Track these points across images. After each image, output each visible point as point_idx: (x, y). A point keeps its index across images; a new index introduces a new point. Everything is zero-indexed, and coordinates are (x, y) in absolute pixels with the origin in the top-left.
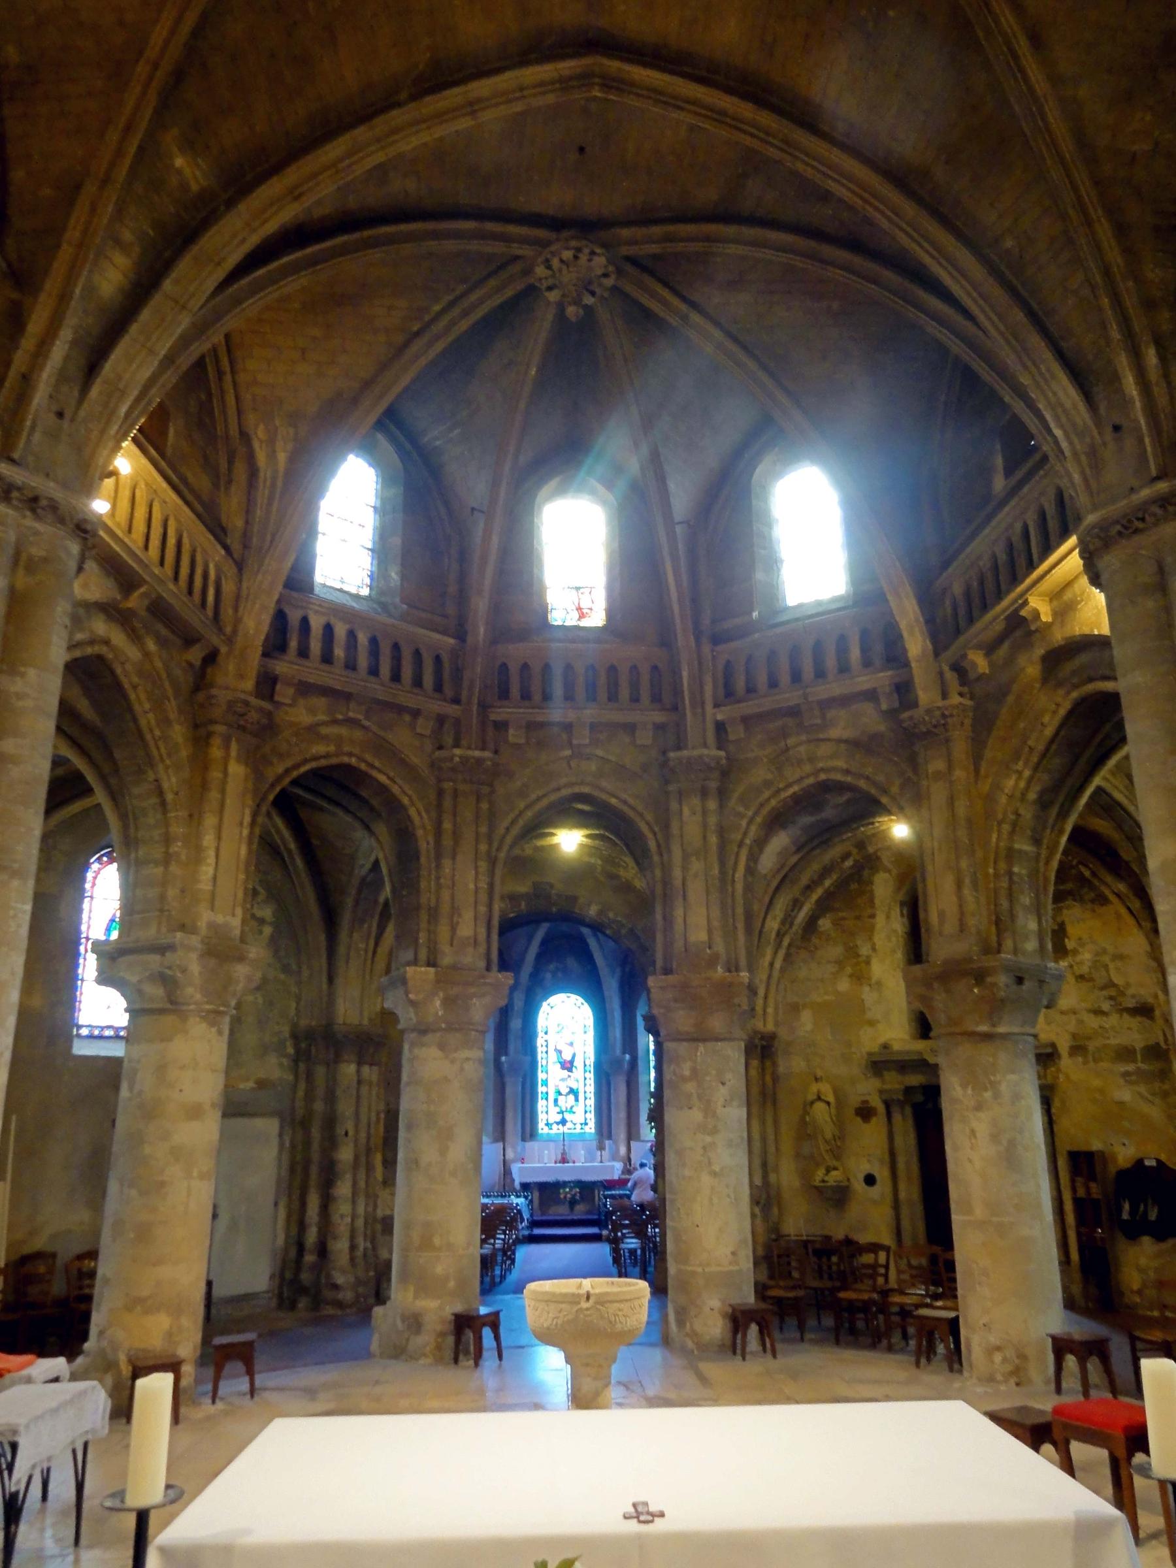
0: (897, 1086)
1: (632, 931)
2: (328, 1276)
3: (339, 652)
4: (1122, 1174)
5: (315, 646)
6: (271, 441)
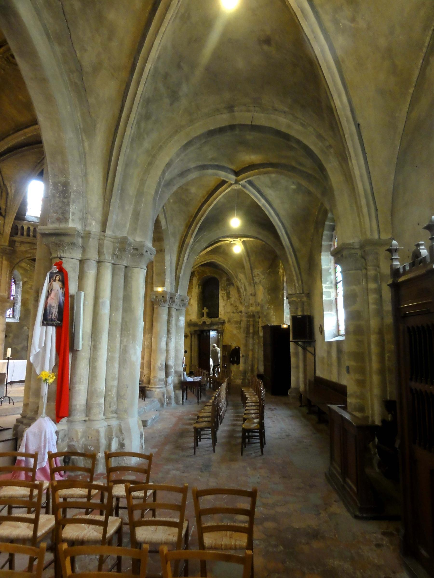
3: (31, 234)
4: (233, 350)
5: (25, 233)
6: (11, 187)
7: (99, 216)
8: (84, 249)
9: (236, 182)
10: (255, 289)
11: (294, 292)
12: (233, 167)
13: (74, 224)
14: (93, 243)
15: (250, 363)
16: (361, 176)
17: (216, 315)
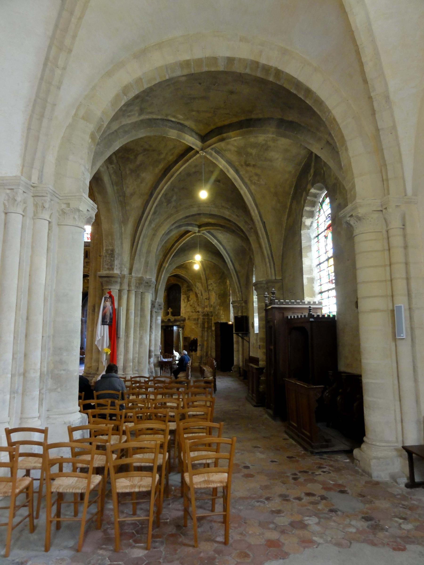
4: (192, 341)
7: (128, 265)
8: (121, 284)
9: (199, 232)
10: (209, 294)
11: (236, 299)
12: (198, 223)
13: (116, 271)
14: (126, 281)
15: (205, 351)
16: (266, 248)
17: (178, 314)
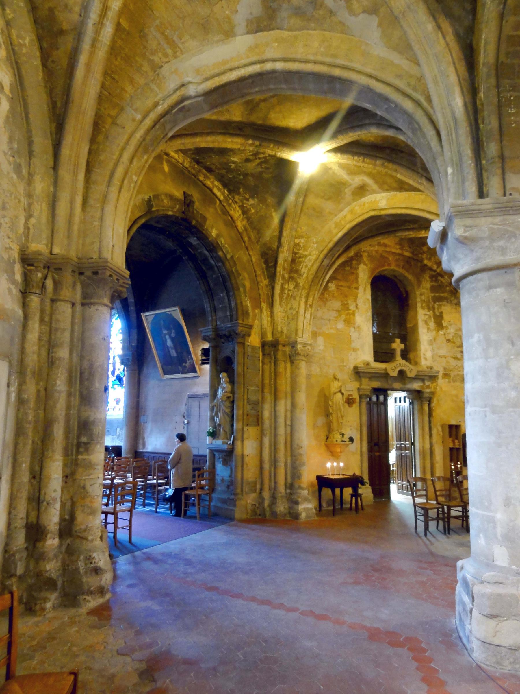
0: (368, 387)
1: (232, 257)
2: (89, 559)
